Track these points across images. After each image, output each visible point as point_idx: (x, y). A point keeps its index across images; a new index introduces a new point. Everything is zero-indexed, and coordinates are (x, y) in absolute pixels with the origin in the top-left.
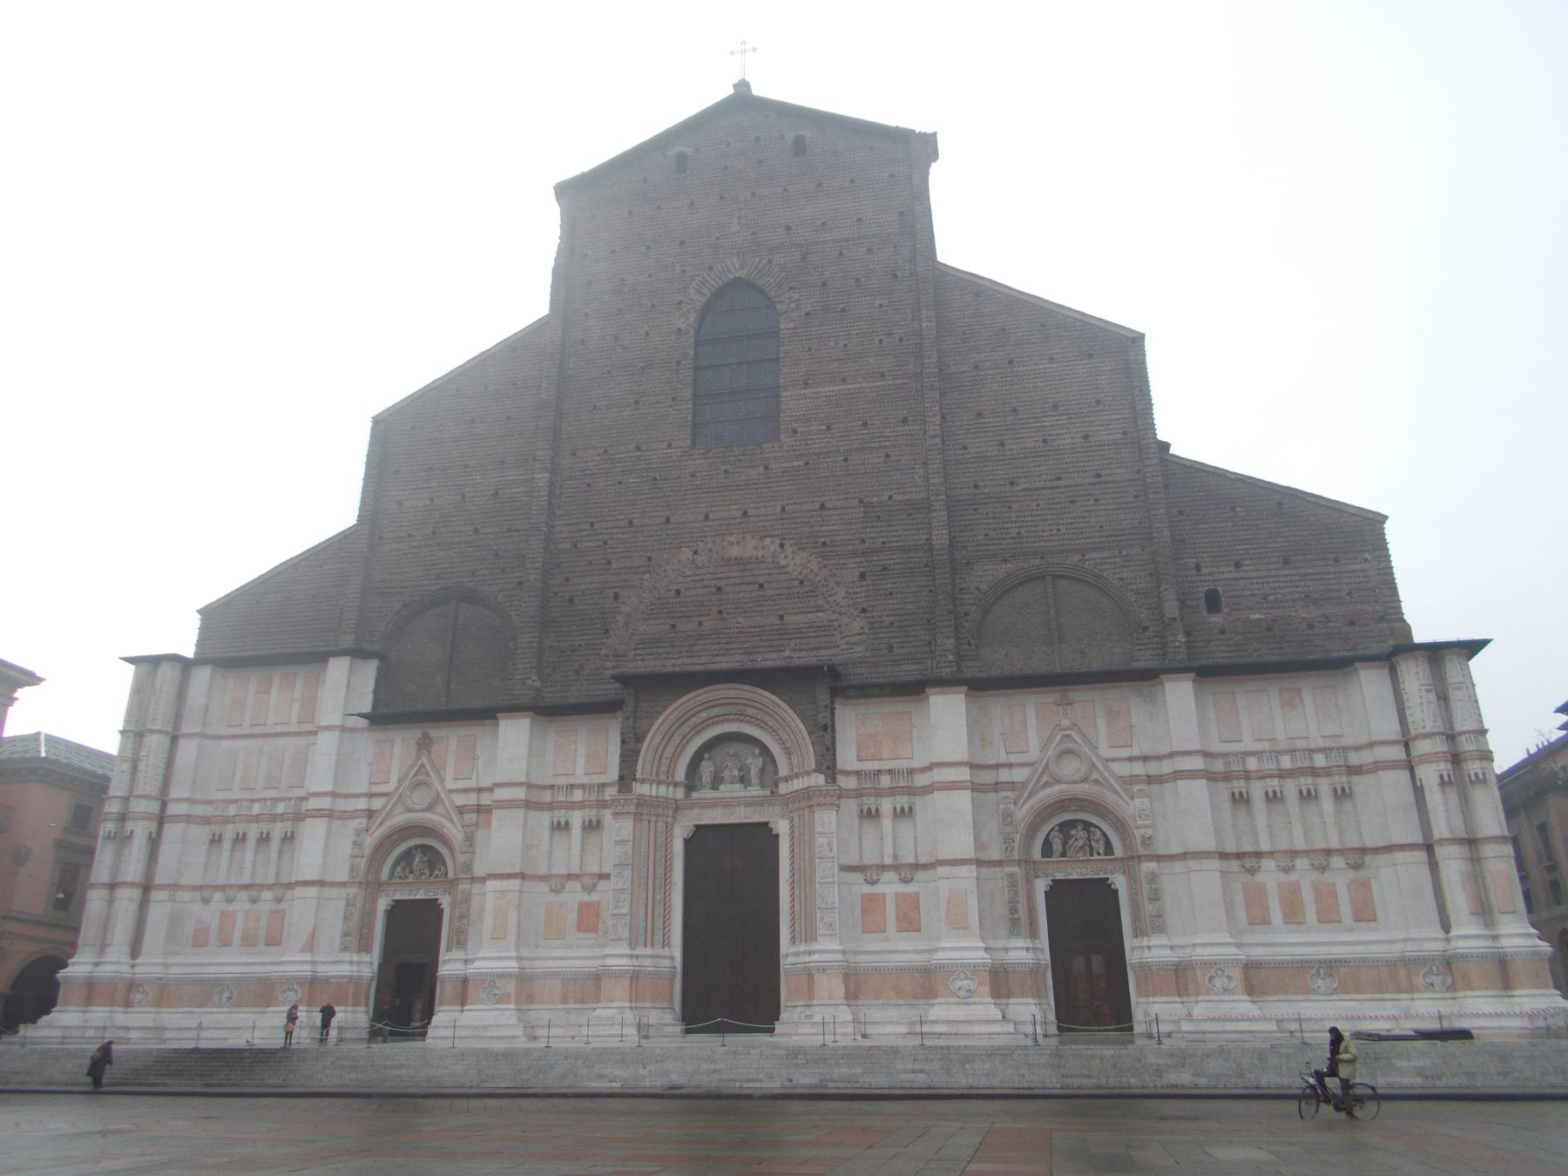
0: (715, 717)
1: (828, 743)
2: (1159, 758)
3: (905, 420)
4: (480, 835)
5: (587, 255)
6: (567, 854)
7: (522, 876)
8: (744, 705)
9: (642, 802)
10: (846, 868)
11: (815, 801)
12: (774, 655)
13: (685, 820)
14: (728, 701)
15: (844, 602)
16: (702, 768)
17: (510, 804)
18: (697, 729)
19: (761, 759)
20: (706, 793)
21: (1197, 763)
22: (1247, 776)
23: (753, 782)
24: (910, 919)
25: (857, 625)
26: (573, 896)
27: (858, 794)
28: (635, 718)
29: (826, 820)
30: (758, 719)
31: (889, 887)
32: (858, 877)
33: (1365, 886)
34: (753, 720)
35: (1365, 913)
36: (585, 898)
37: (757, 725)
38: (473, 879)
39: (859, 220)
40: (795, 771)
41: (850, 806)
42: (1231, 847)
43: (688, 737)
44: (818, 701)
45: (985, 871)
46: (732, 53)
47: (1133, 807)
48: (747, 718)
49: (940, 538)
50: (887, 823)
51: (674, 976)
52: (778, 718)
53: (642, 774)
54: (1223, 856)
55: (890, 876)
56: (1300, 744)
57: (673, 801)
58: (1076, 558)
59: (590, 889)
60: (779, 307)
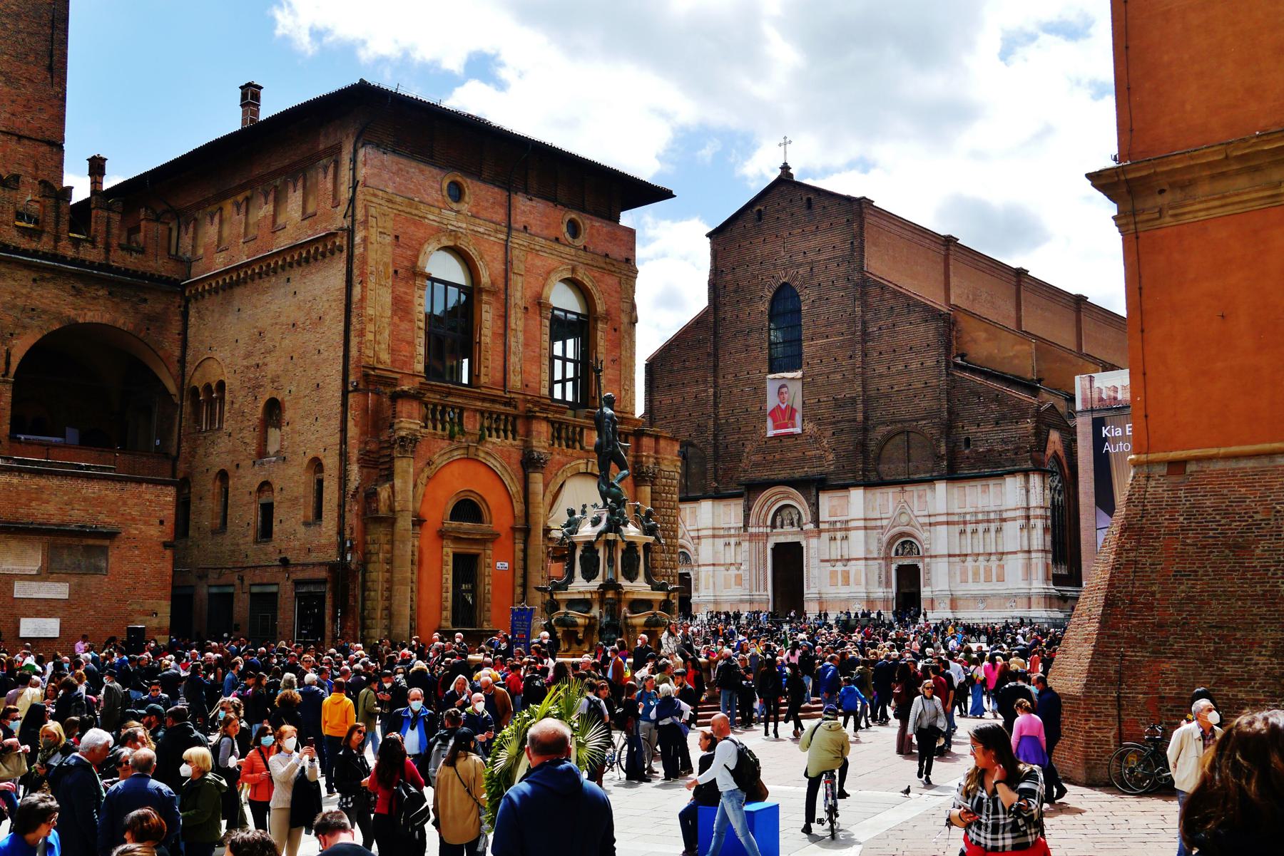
2: (935, 515)
3: (851, 357)
4: (700, 547)
5: (722, 271)
6: (730, 555)
7: (714, 565)
9: (751, 535)
10: (823, 561)
12: (801, 470)
15: (827, 446)
17: (706, 537)
20: (779, 530)
21: (944, 519)
22: (965, 523)
24: (846, 582)
25: (831, 457)
26: (733, 571)
27: (828, 531)
29: (814, 542)
31: (839, 567)
32: (828, 564)
33: (1003, 567)
35: (1001, 579)
36: (737, 572)
38: (699, 566)
39: (834, 247)
41: (825, 536)
42: (958, 553)
45: (870, 562)
46: (780, 145)
47: (923, 535)
49: (860, 417)
50: (839, 542)
51: (768, 603)
54: (950, 556)
55: (839, 564)
56: (986, 509)
58: (915, 424)
59: (738, 569)
60: (801, 298)
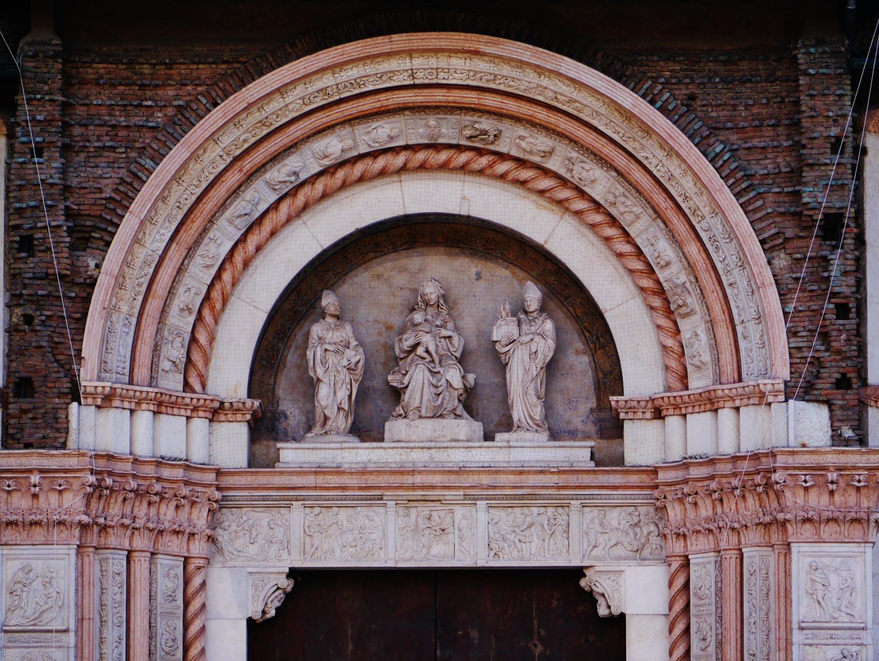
0: (374, 155)
1: (843, 286)
8: (500, 115)
11: (793, 499)
13: (253, 549)
14: (439, 96)
16: (314, 353)
18: (301, 198)
19: (549, 326)
23: (518, 413)
28: (66, 149)
30: (546, 172)
34: (526, 174)
37: (541, 192)
40: (698, 382)
43: (267, 226)
44: (805, 123)
48: (502, 167)
52: (638, 175)
53: (103, 367)
57: (210, 477)
